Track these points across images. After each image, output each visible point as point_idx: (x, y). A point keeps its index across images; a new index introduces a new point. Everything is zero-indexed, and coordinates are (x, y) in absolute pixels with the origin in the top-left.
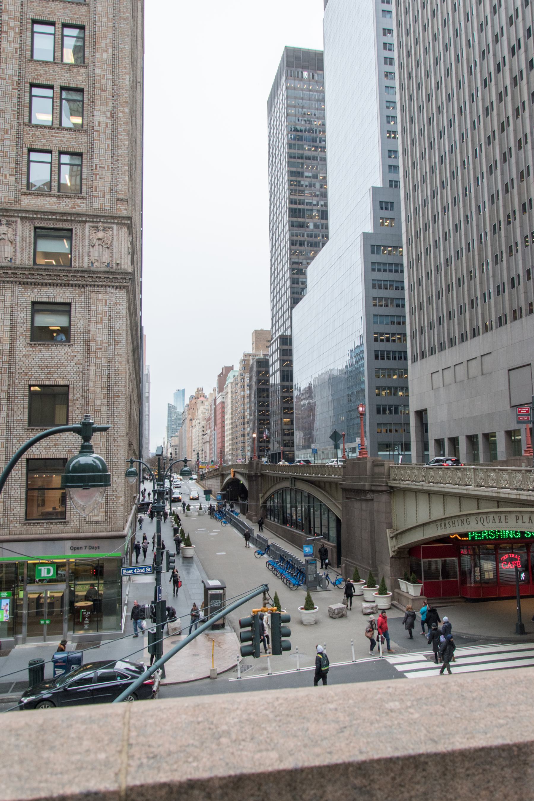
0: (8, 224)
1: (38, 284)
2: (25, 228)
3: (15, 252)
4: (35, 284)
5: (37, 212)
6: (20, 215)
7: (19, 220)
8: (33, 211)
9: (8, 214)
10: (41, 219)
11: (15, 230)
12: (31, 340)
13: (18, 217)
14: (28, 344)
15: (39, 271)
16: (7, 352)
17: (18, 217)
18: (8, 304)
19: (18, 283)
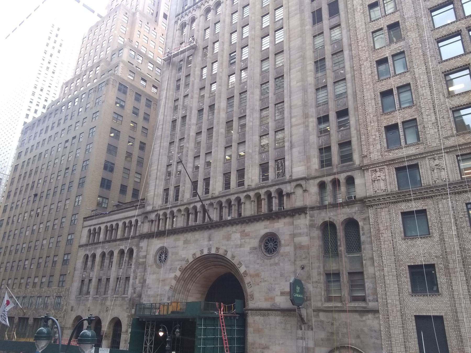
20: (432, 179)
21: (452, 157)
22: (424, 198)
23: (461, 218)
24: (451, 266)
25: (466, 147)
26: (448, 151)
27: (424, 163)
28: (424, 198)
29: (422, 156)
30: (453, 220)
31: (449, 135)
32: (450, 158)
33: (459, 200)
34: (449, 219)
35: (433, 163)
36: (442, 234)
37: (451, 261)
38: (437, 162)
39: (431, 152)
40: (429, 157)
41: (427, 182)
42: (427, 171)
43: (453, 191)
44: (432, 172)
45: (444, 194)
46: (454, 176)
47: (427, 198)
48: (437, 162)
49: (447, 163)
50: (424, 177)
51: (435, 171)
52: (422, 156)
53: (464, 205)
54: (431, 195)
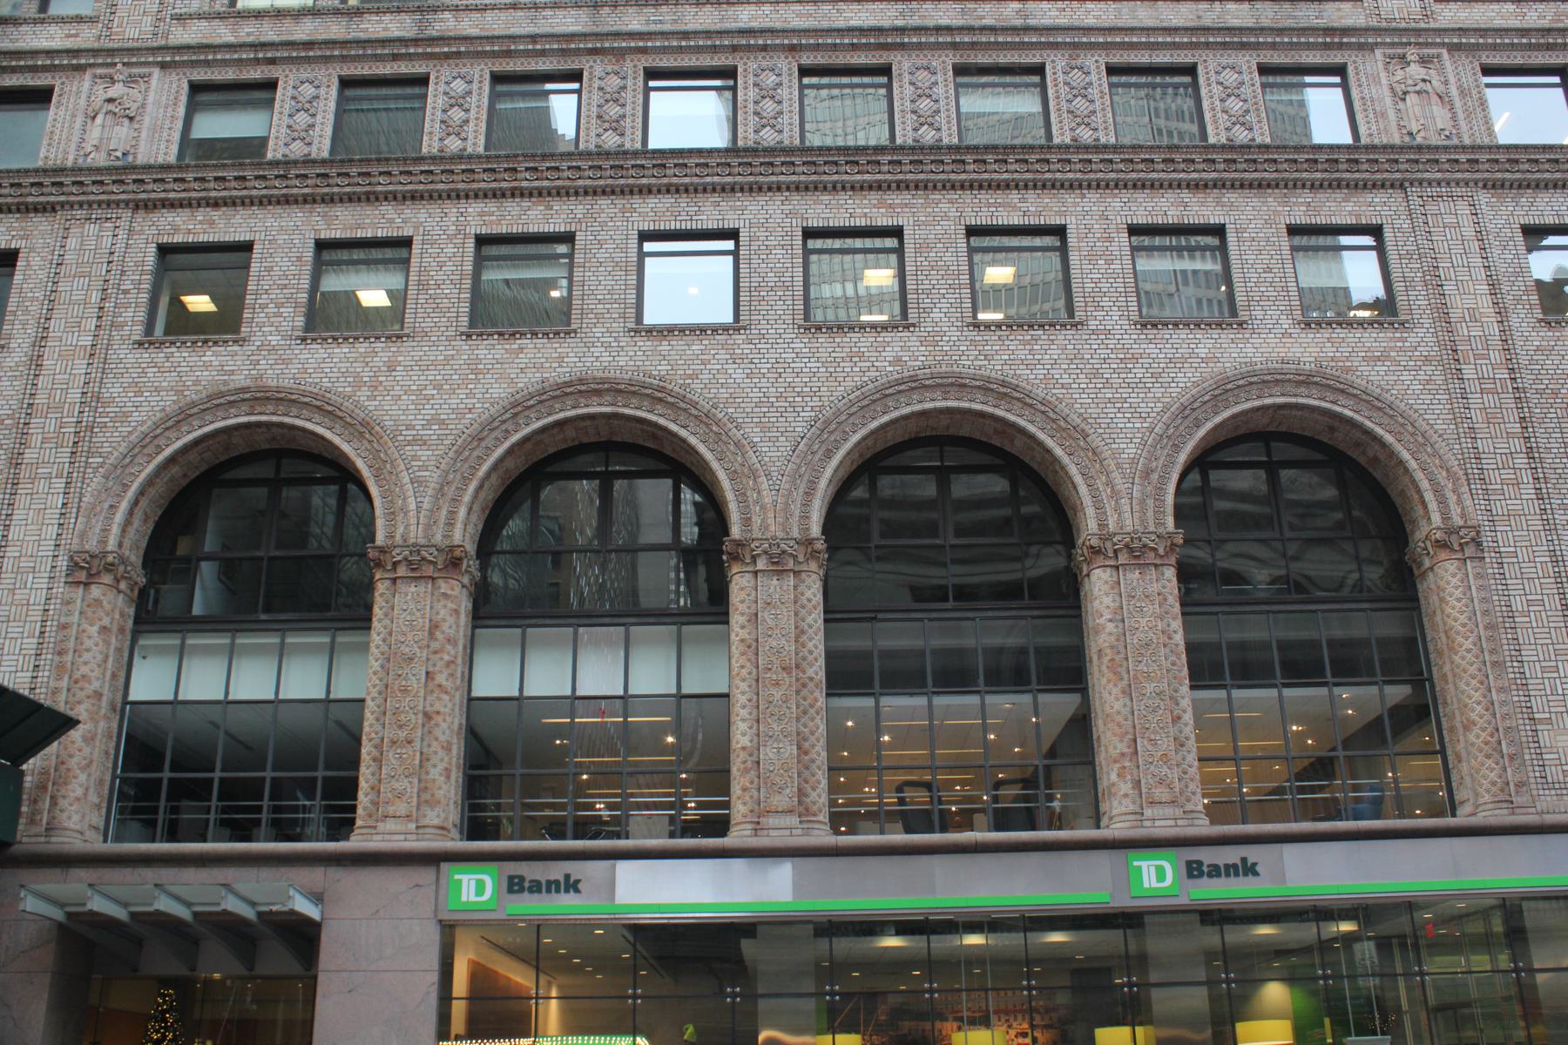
0: (1424, 61)
1: (1528, 186)
2: (1461, 68)
3: (1454, 118)
4: (1520, 187)
5: (1486, 30)
6: (1446, 40)
7: (1444, 52)
8: (1475, 30)
9: (1421, 40)
10: (1495, 47)
11: (1441, 71)
12: (1544, 313)
13: (1443, 45)
14: (1540, 321)
15: (1530, 153)
16: (1496, 342)
17: (1443, 45)
18: (1469, 232)
19: (1480, 184)
20: (79, 148)
21: (174, 86)
22: (25, 209)
23: (126, 292)
24: (30, 455)
25: (228, 57)
26: (168, 59)
27: (74, 88)
28: (28, 211)
29: (75, 61)
30: (95, 297)
31: (192, 10)
32: (166, 86)
33: (142, 232)
34: (79, 292)
35: (101, 93)
36: (41, 340)
37: (36, 440)
38: (116, 90)
39: (111, 52)
40: (99, 71)
41: (60, 156)
42: (74, 116)
43: (131, 196)
44: (89, 121)
45: (100, 203)
46: (154, 147)
47: (36, 210)
48: (116, 90)
49: (151, 99)
50: (56, 138)
51: (99, 120)
52: (74, 62)
53: (152, 249)
54: (52, 199)
